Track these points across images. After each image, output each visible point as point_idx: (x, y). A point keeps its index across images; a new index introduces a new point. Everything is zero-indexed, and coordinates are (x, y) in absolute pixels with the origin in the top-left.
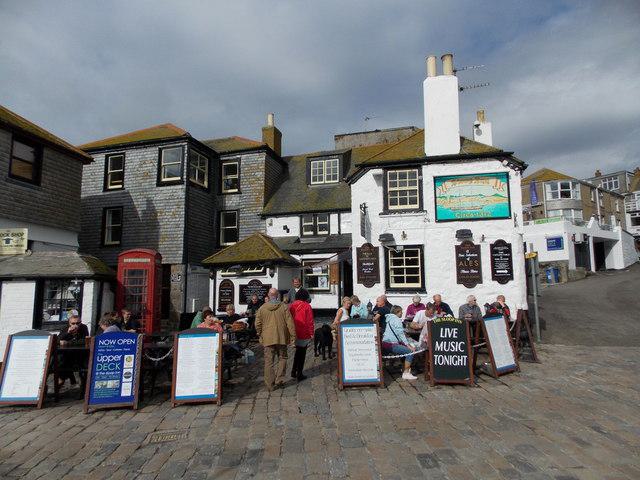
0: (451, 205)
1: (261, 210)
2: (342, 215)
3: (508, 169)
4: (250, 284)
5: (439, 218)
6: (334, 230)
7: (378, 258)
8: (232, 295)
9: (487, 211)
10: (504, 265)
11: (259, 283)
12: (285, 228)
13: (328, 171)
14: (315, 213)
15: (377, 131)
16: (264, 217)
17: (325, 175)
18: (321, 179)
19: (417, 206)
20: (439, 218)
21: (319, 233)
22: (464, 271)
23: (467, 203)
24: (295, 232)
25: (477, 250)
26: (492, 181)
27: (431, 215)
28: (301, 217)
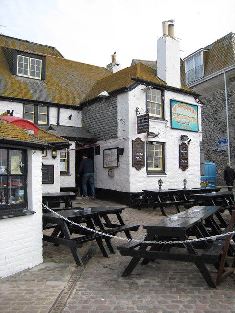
0: (179, 120)
2: (62, 110)
5: (173, 127)
6: (53, 121)
13: (33, 68)
14: (37, 103)
15: (27, 41)
17: (29, 70)
19: (159, 116)
20: (173, 127)
23: (183, 120)
27: (169, 124)
28: (24, 104)
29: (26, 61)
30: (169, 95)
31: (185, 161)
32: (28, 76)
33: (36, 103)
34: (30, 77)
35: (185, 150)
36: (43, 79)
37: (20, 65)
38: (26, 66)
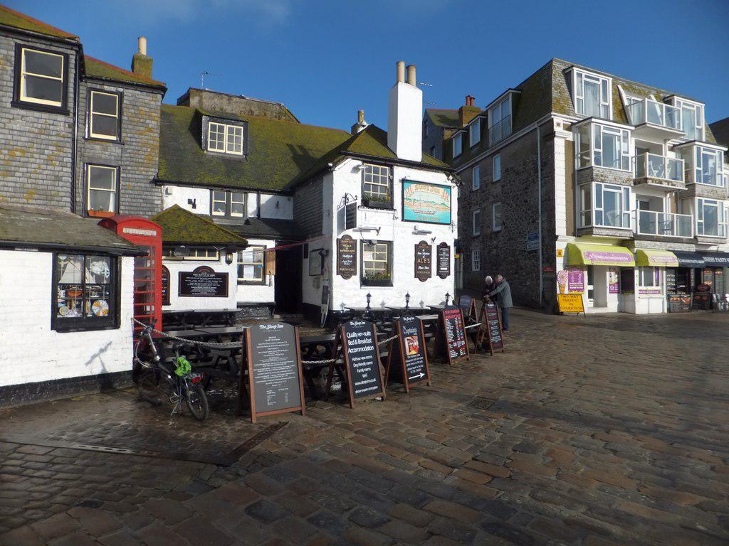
1: (152, 173)
3: (449, 183)
4: (197, 270)
7: (356, 251)
8: (166, 284)
9: (436, 217)
11: (211, 271)
12: (190, 202)
13: (230, 139)
16: (158, 182)
17: (226, 142)
20: (405, 218)
21: (232, 215)
22: (420, 268)
23: (424, 209)
24: (203, 208)
25: (429, 249)
26: (441, 190)
27: (399, 214)
28: (211, 190)
29: (221, 129)
30: (400, 172)
31: (426, 268)
33: (228, 189)
35: (426, 252)
37: (213, 136)
38: (221, 137)
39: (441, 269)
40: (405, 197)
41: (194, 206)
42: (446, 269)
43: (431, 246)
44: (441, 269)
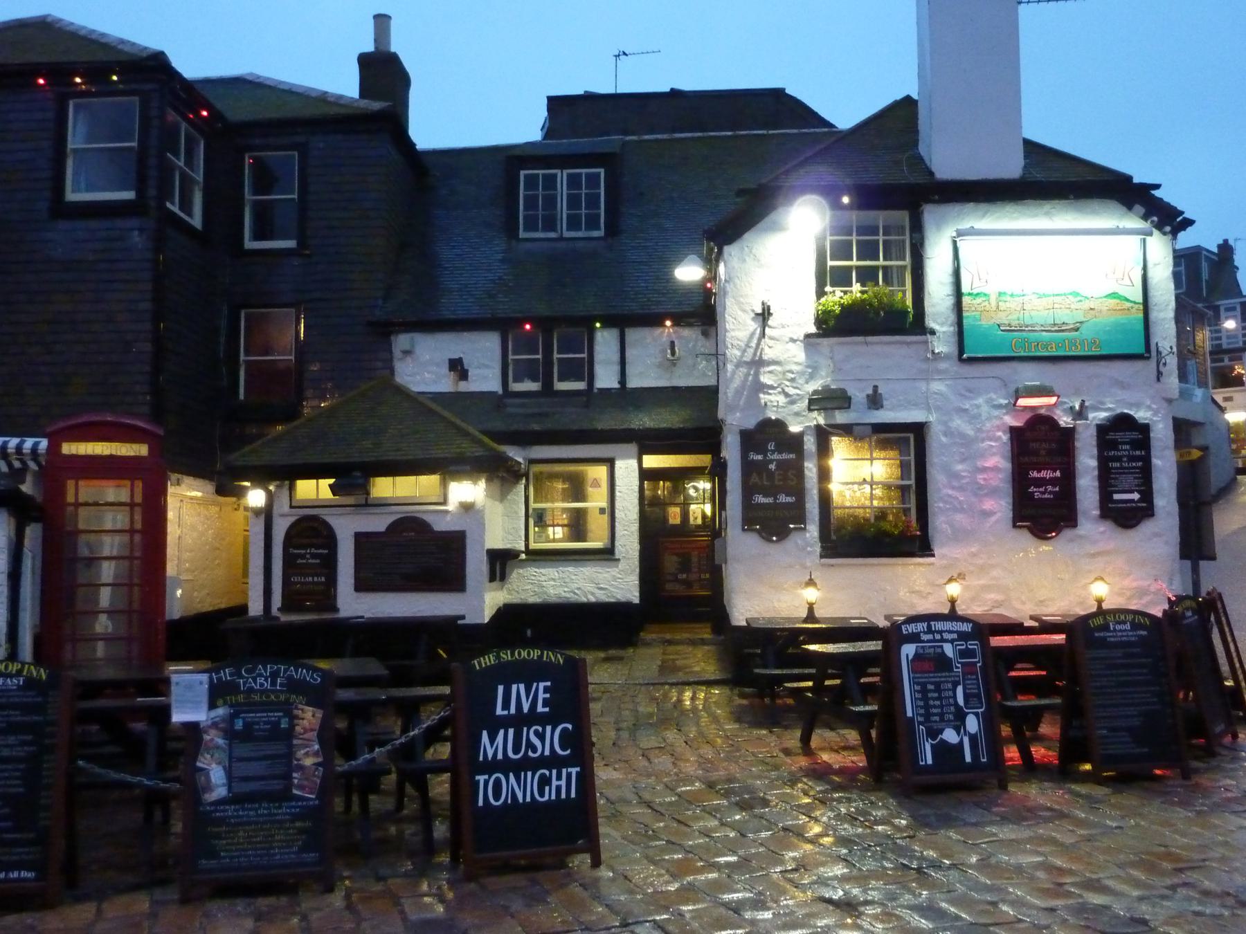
2: (633, 334)
6: (606, 378)
8: (329, 564)
10: (1130, 480)
13: (573, 202)
18: (550, 224)
27: (943, 344)
29: (550, 182)
32: (552, 235)
34: (567, 234)
36: (613, 229)
38: (551, 202)
39: (1116, 497)
40: (965, 288)
41: (463, 375)
42: (1136, 496)
43: (1069, 433)
44: (1116, 497)
